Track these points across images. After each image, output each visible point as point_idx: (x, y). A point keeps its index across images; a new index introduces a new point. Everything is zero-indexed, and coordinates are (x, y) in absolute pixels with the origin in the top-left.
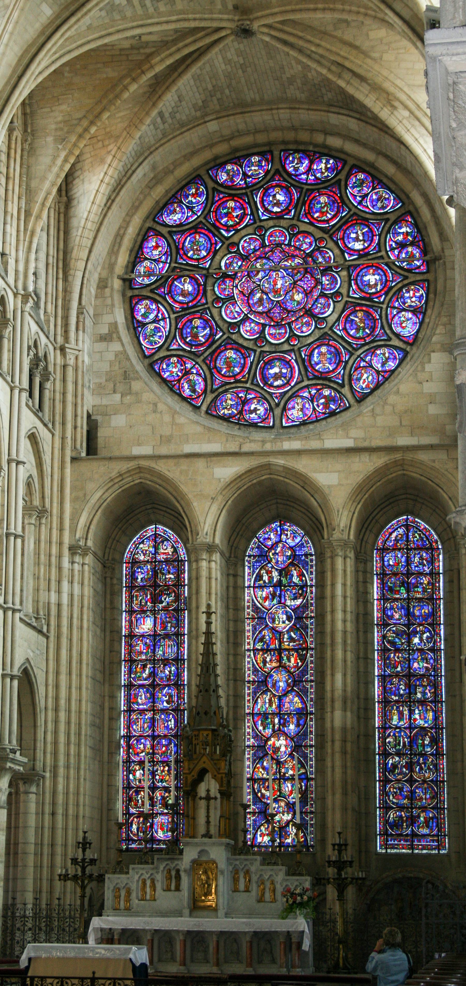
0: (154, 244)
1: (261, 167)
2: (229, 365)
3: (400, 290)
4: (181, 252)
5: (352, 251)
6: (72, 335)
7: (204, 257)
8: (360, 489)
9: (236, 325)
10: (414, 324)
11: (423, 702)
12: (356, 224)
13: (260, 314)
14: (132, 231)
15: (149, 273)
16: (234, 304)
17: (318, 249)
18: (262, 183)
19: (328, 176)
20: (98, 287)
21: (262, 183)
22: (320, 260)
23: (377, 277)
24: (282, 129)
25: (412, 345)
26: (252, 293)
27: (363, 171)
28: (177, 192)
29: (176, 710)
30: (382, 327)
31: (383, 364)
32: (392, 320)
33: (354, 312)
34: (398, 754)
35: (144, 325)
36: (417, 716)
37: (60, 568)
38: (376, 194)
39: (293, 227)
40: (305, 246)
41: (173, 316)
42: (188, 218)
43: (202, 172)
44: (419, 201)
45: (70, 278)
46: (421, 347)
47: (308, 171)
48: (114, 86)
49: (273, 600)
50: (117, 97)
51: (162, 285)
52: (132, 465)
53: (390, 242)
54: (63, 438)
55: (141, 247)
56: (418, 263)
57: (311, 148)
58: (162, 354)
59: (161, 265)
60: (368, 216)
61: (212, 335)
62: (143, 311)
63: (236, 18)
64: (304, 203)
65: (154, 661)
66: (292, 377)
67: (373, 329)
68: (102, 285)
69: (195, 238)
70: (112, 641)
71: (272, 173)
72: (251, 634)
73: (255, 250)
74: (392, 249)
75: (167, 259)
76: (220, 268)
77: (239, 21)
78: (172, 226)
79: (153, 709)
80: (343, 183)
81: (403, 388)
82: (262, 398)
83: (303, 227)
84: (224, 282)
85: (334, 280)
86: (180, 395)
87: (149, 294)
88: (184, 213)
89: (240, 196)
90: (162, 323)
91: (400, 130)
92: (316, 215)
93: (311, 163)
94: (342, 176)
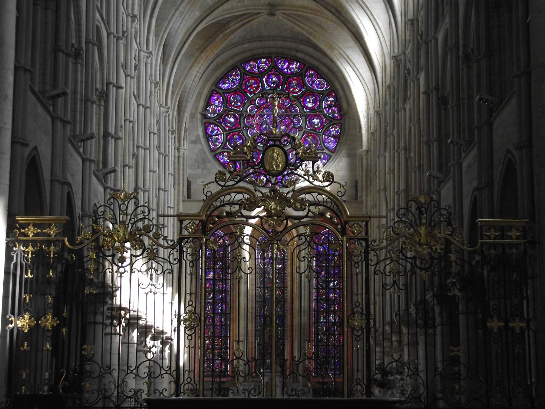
0: (216, 98)
1: (266, 64)
3: (329, 127)
4: (229, 102)
5: (307, 108)
6: (182, 142)
7: (240, 106)
10: (334, 143)
11: (334, 312)
12: (309, 95)
14: (206, 92)
15: (214, 112)
16: (253, 129)
17: (292, 105)
18: (266, 72)
19: (297, 71)
20: (190, 117)
21: (266, 72)
22: (293, 111)
23: (318, 120)
24: (277, 47)
25: (333, 153)
26: (262, 125)
28: (227, 73)
30: (320, 144)
32: (325, 141)
33: (308, 136)
34: (323, 334)
36: (332, 318)
38: (319, 81)
40: (286, 104)
41: (225, 133)
42: (232, 86)
44: (338, 87)
45: (181, 116)
46: (338, 154)
47: (288, 68)
49: (268, 265)
54: (178, 191)
56: (337, 115)
57: (289, 57)
58: (220, 150)
59: (219, 108)
60: (315, 91)
62: (211, 130)
63: (269, 8)
64: (286, 84)
68: (192, 116)
69: (235, 96)
71: (271, 68)
72: (259, 280)
73: (263, 104)
74: (325, 108)
75: (222, 105)
76: (247, 111)
77: (270, 9)
78: (224, 90)
80: (304, 75)
84: (249, 118)
85: (299, 121)
87: (214, 122)
88: (230, 84)
90: (220, 136)
91: (335, 59)
92: (291, 89)
94: (303, 71)
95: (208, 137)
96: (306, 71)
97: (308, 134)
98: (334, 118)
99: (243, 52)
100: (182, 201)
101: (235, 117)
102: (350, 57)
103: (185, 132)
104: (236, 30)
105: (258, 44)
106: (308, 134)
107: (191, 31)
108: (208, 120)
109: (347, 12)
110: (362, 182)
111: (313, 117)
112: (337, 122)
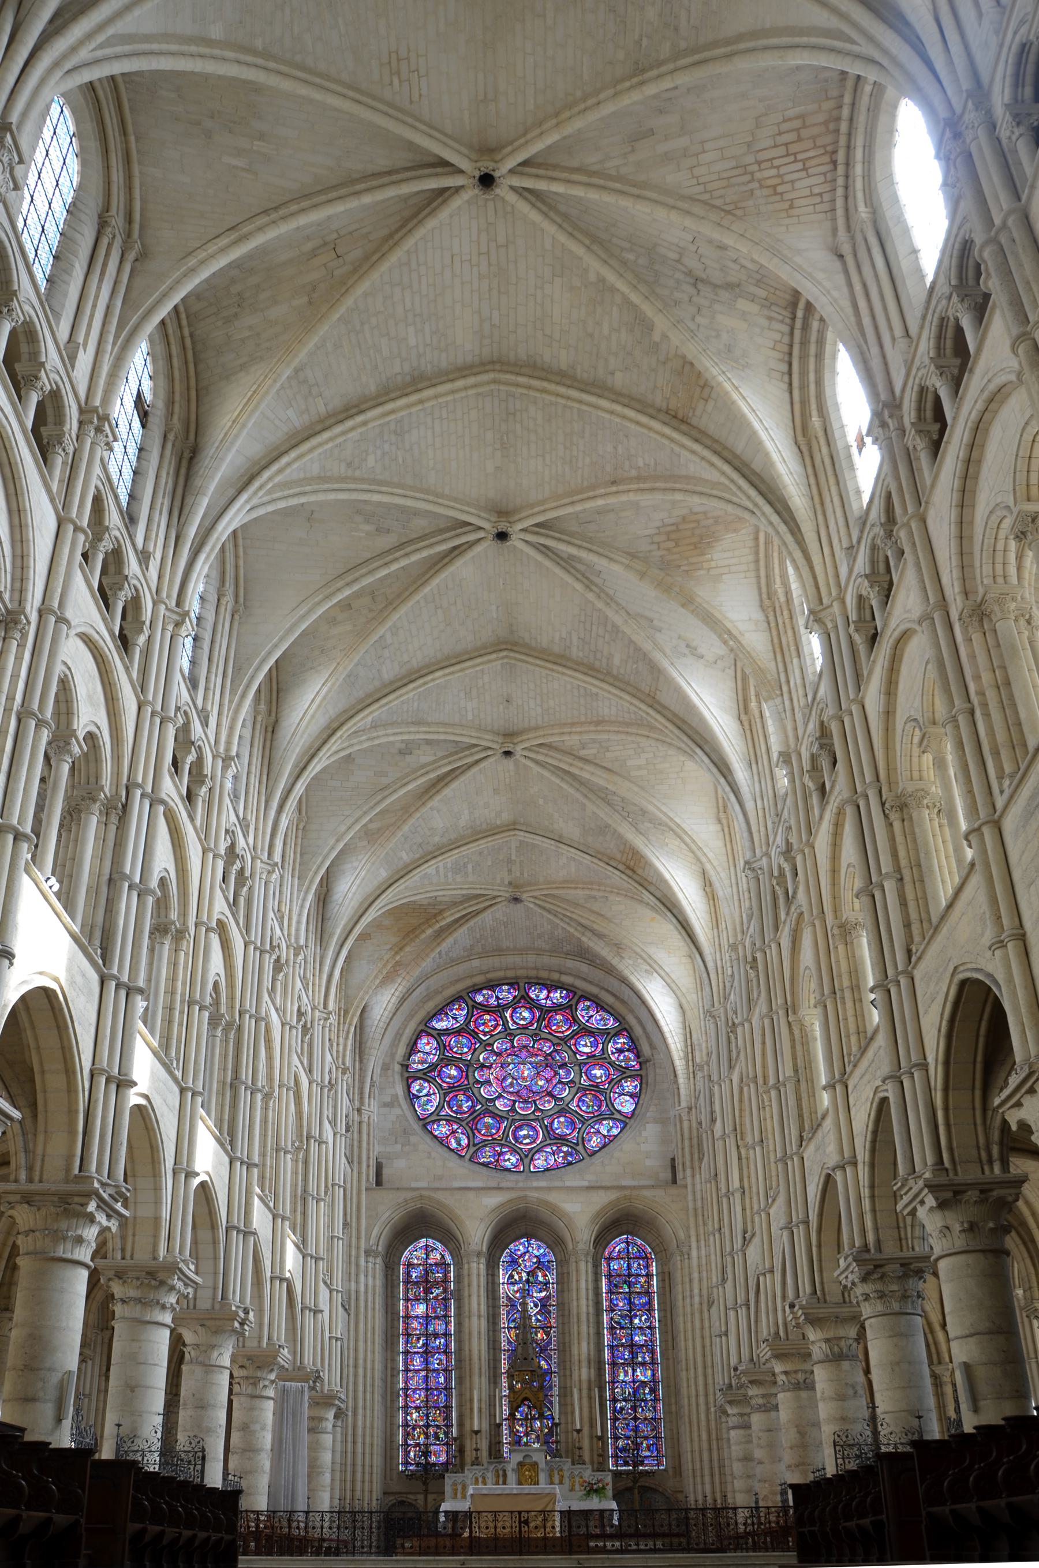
2: (488, 1127)
5: (582, 1053)
8: (597, 1215)
9: (493, 1100)
13: (512, 1093)
16: (491, 1085)
26: (505, 1079)
29: (445, 1370)
33: (585, 1095)
35: (418, 1097)
37: (358, 1265)
51: (433, 1070)
53: (610, 1048)
54: (359, 1173)
58: (433, 1118)
61: (473, 1106)
65: (427, 1335)
67: (600, 1107)
70: (393, 1320)
79: (427, 1369)
85: (568, 1073)
95: (412, 1098)
97: (585, 1090)
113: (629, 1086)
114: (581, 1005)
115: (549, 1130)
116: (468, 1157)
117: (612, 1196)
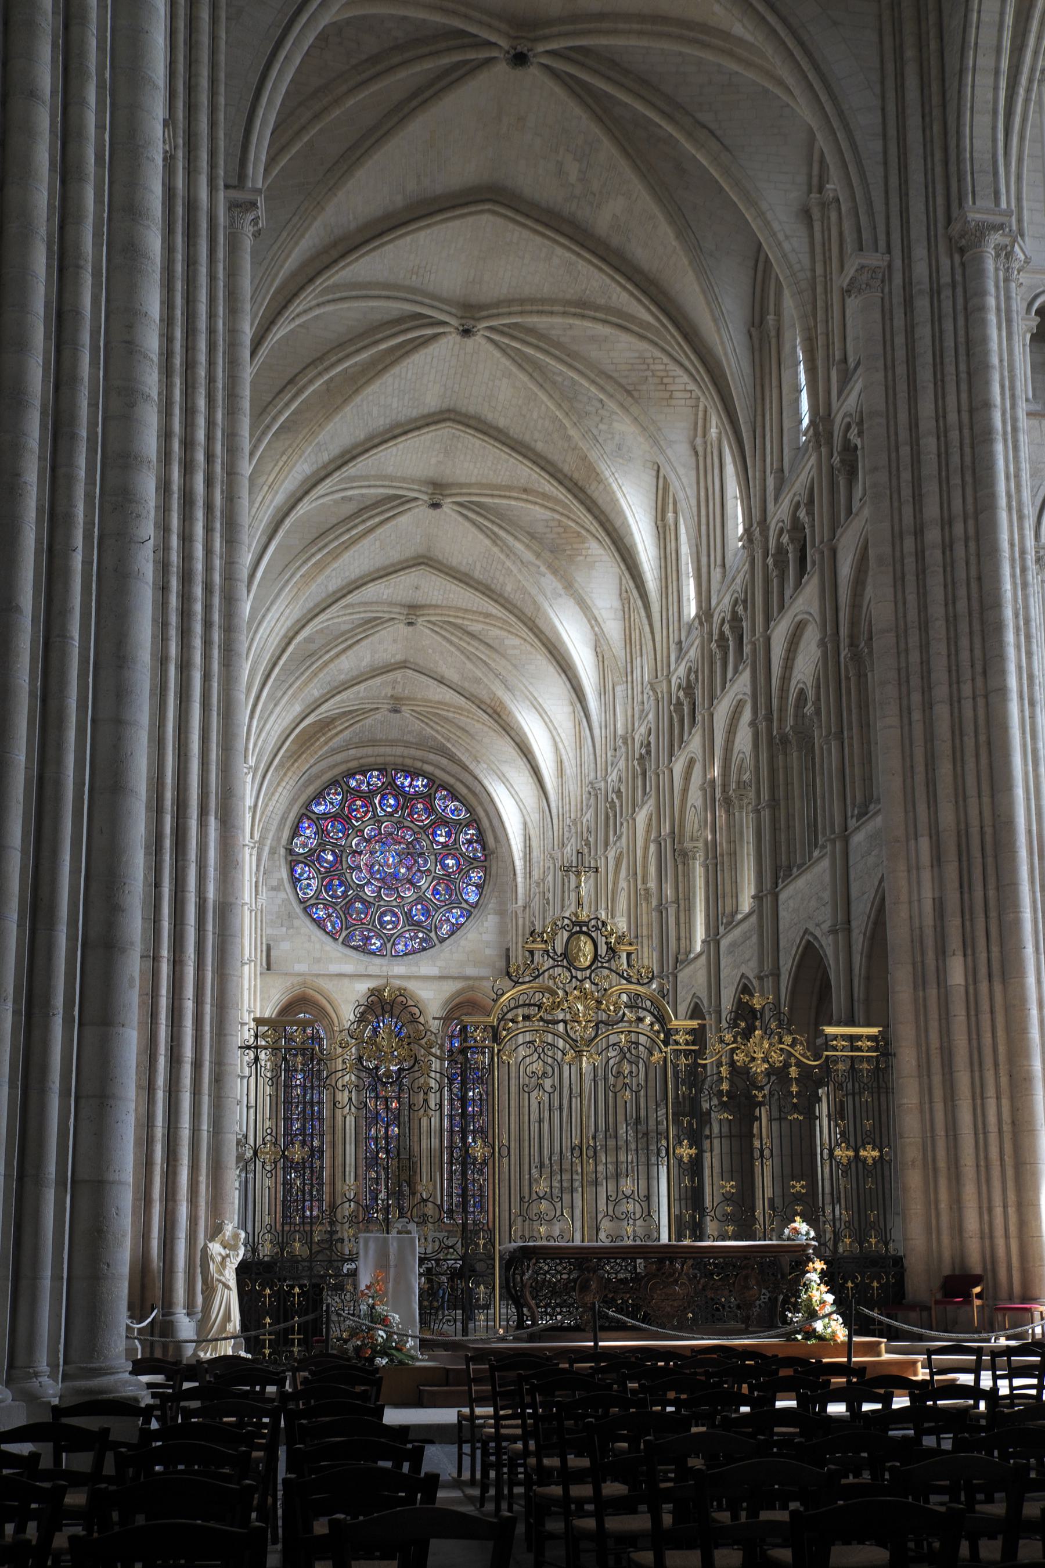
1: (379, 779)
2: (359, 913)
5: (438, 843)
8: (448, 1002)
9: (362, 887)
14: (292, 816)
15: (304, 845)
16: (361, 871)
26: (373, 866)
27: (446, 789)
31: (457, 920)
33: (438, 884)
39: (400, 822)
43: (339, 778)
44: (482, 814)
47: (410, 785)
48: (311, 738)
50: (312, 745)
51: (312, 855)
52: (300, 979)
53: (462, 838)
55: (297, 827)
62: (299, 871)
64: (407, 807)
66: (398, 923)
67: (451, 896)
68: (273, 852)
73: (375, 836)
74: (464, 844)
81: (470, 936)
82: (379, 937)
83: (407, 824)
85: (426, 862)
86: (325, 930)
89: (365, 798)
93: (412, 780)
94: (432, 791)
95: (295, 881)
96: (436, 792)
97: (440, 879)
98: (475, 859)
99: (347, 762)
100: (261, 974)
101: (334, 853)
102: (507, 775)
103: (264, 874)
104: (341, 731)
105: (369, 751)
106: (440, 879)
107: (288, 732)
108: (294, 858)
109: (510, 713)
110: (517, 950)
111: (446, 856)
112: (480, 864)
113: (476, 876)
114: (438, 795)
115: (408, 915)
116: (341, 940)
117: (458, 985)
